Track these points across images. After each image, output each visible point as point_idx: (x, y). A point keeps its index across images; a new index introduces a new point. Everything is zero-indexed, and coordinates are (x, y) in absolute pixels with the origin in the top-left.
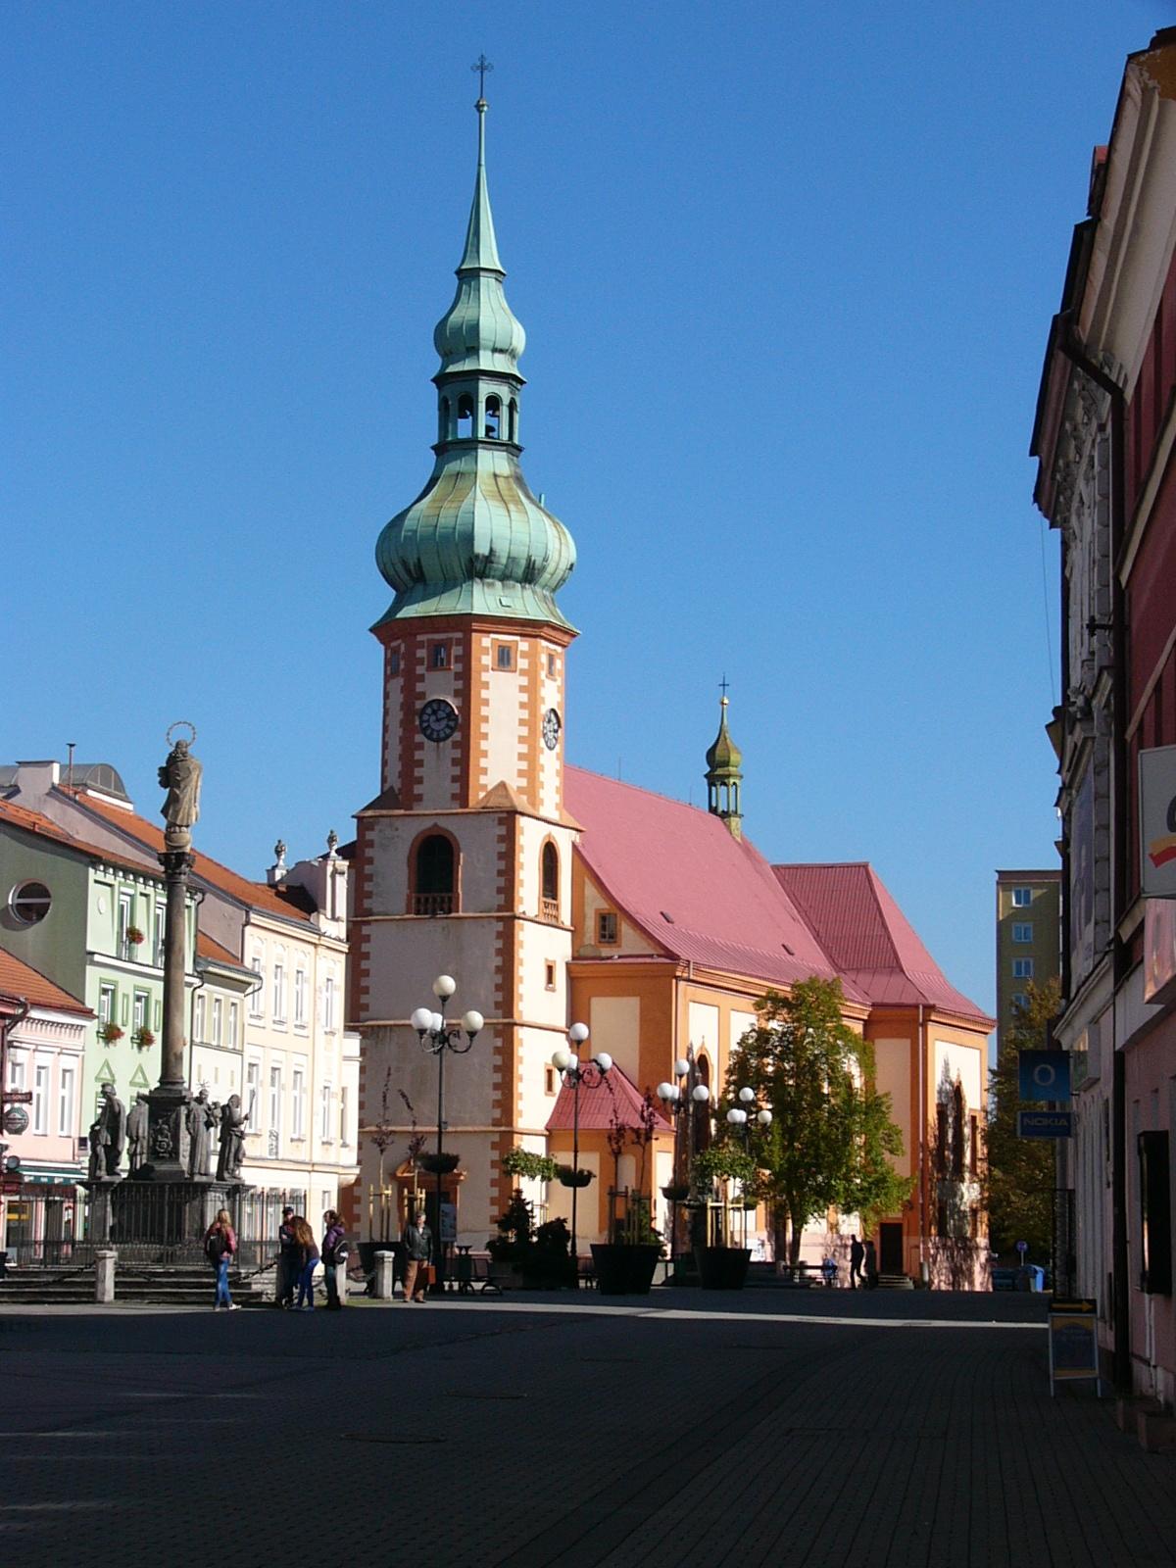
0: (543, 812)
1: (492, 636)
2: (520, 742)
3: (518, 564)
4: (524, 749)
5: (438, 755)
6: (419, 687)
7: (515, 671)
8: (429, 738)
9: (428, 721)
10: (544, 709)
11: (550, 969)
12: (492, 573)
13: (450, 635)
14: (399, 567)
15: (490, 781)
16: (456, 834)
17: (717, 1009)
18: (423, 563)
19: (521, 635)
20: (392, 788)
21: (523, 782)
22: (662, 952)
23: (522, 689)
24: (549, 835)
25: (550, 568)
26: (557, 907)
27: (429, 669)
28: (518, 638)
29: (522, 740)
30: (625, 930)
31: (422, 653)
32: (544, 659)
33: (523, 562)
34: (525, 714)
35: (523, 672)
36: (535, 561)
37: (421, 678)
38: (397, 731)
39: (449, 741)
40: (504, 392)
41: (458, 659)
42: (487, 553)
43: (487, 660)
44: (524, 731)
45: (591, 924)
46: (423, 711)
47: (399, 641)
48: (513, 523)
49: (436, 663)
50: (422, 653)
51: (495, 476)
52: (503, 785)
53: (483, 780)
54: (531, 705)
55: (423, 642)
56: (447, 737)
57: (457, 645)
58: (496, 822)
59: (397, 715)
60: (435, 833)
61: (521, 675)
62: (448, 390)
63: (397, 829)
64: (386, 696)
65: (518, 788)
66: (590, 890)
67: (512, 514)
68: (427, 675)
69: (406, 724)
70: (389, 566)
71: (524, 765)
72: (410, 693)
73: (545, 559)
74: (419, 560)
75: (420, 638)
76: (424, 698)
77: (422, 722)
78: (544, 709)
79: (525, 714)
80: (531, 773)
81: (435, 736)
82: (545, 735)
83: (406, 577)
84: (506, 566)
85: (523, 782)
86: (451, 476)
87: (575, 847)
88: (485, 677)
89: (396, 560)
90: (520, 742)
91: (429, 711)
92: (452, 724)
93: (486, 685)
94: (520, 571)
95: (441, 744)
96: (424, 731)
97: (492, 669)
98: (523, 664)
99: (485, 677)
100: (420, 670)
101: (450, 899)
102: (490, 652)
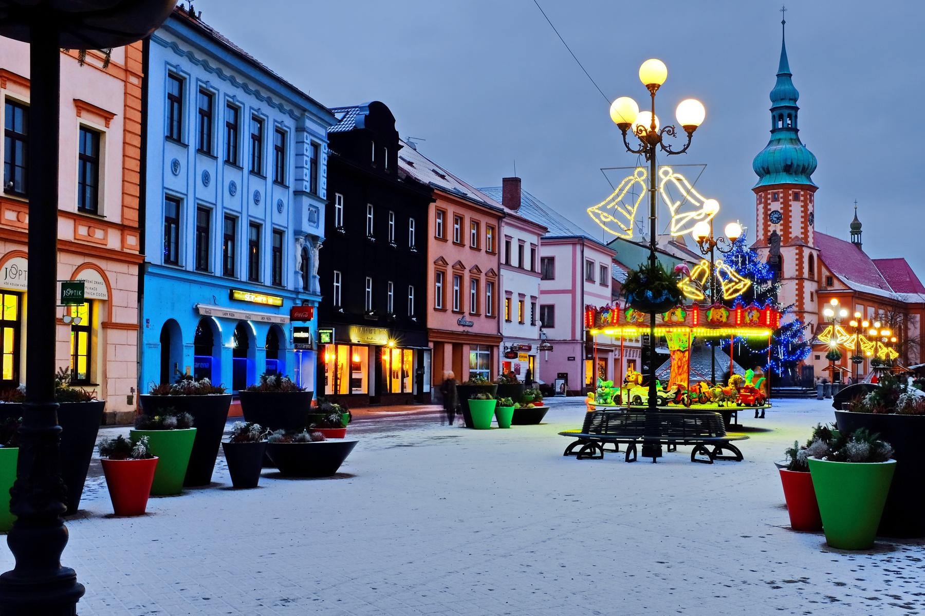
1: (792, 190)
4: (803, 225)
6: (769, 207)
8: (773, 223)
10: (809, 212)
11: (812, 294)
13: (778, 190)
14: (761, 169)
15: (792, 236)
17: (862, 307)
20: (760, 239)
21: (803, 236)
22: (847, 288)
23: (802, 206)
24: (811, 252)
25: (810, 168)
26: (813, 275)
28: (800, 190)
29: (802, 222)
30: (836, 282)
31: (769, 196)
32: (808, 196)
33: (802, 166)
34: (803, 214)
35: (802, 201)
37: (770, 204)
38: (761, 221)
39: (779, 224)
40: (793, 112)
41: (781, 198)
42: (790, 164)
43: (791, 198)
44: (803, 220)
45: (824, 280)
46: (770, 215)
49: (775, 199)
50: (769, 196)
52: (797, 237)
53: (790, 236)
54: (805, 210)
59: (761, 216)
62: (775, 113)
64: (757, 210)
66: (824, 270)
68: (771, 203)
69: (765, 219)
70: (758, 169)
71: (803, 231)
72: (766, 209)
73: (809, 165)
74: (768, 167)
75: (769, 191)
77: (770, 218)
78: (809, 212)
79: (803, 214)
80: (806, 233)
83: (763, 172)
84: (797, 167)
85: (803, 236)
87: (818, 255)
88: (790, 203)
89: (760, 166)
91: (772, 214)
93: (791, 206)
94: (801, 170)
96: (771, 221)
98: (802, 198)
99: (790, 203)
100: (769, 202)
101: (781, 273)
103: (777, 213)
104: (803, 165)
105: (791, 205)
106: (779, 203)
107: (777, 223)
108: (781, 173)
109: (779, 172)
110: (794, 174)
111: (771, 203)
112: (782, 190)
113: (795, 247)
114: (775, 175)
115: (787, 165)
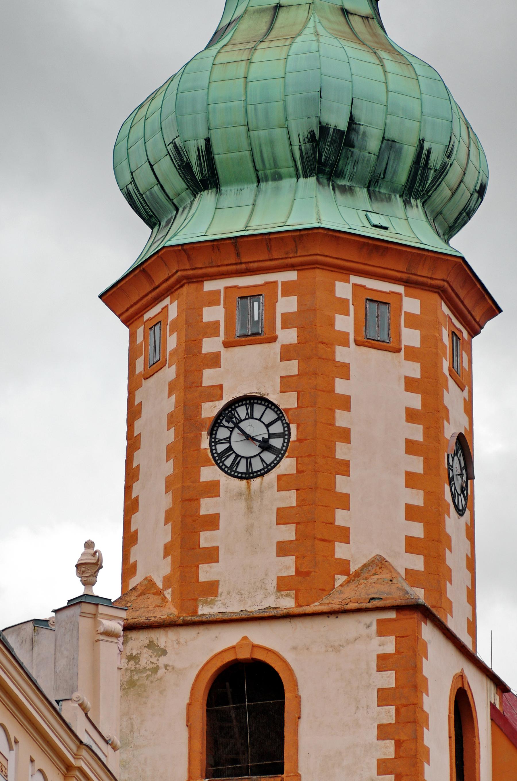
0: (451, 624)
1: (355, 279)
2: (408, 485)
3: (399, 152)
5: (250, 509)
7: (398, 351)
9: (228, 440)
12: (348, 169)
16: (289, 657)
18: (216, 148)
19: (407, 283)
20: (149, 583)
27: (227, 345)
28: (400, 289)
36: (429, 151)
39: (271, 477)
46: (216, 423)
47: (167, 301)
48: (389, 75)
51: (345, 12)
55: (218, 292)
56: (268, 468)
57: (285, 294)
58: (374, 627)
60: (244, 655)
61: (407, 358)
63: (164, 652)
65: (406, 570)
67: (386, 62)
68: (226, 355)
74: (208, 141)
75: (209, 286)
76: (221, 398)
77: (214, 442)
81: (242, 468)
82: (451, 480)
84: (379, 156)
86: (262, 11)
90: (408, 485)
92: (277, 443)
95: (256, 483)
97: (358, 343)
102: (351, 308)
103: (258, 409)
104: (421, 142)
105: (346, 367)
106: (276, 348)
107: (261, 474)
108: (287, 183)
109: (278, 177)
110: (362, 193)
111: (226, 355)
112: (292, 276)
113: (372, 619)
114: (250, 189)
115: (324, 129)
